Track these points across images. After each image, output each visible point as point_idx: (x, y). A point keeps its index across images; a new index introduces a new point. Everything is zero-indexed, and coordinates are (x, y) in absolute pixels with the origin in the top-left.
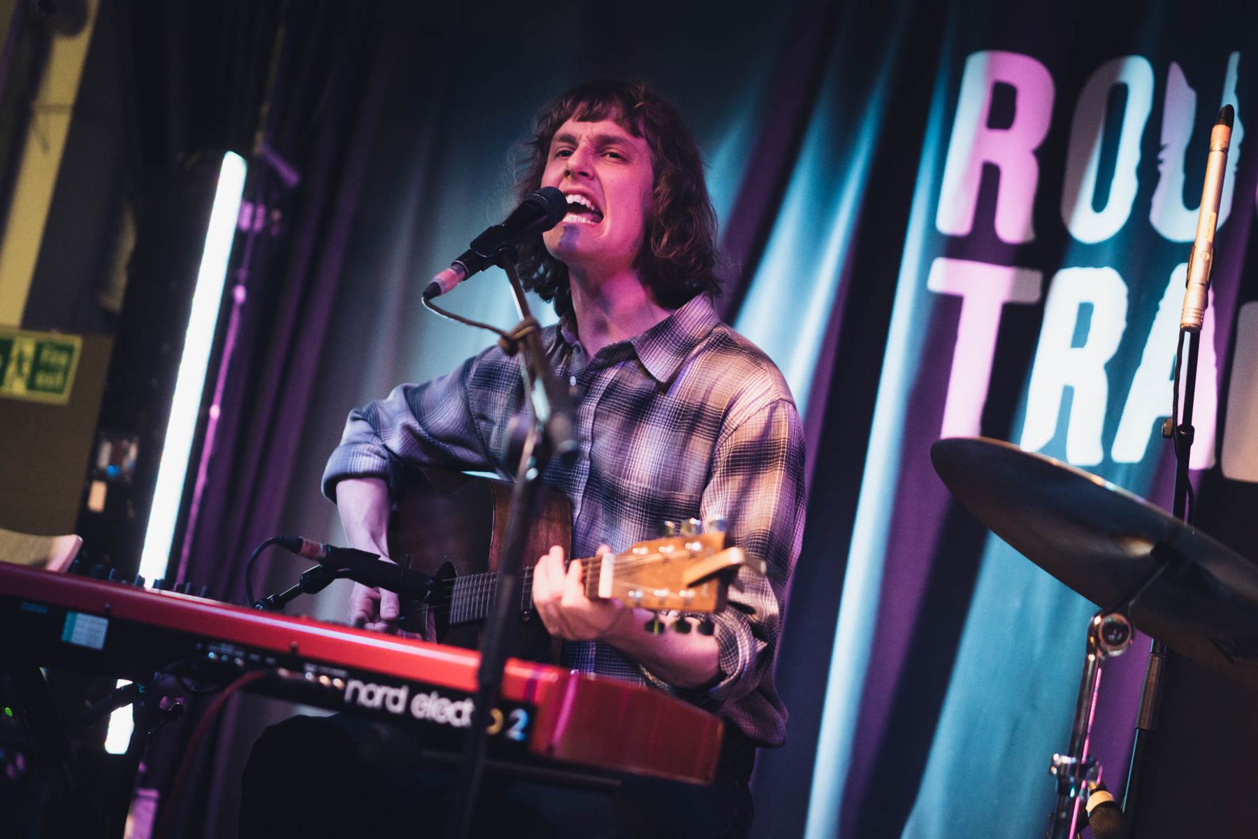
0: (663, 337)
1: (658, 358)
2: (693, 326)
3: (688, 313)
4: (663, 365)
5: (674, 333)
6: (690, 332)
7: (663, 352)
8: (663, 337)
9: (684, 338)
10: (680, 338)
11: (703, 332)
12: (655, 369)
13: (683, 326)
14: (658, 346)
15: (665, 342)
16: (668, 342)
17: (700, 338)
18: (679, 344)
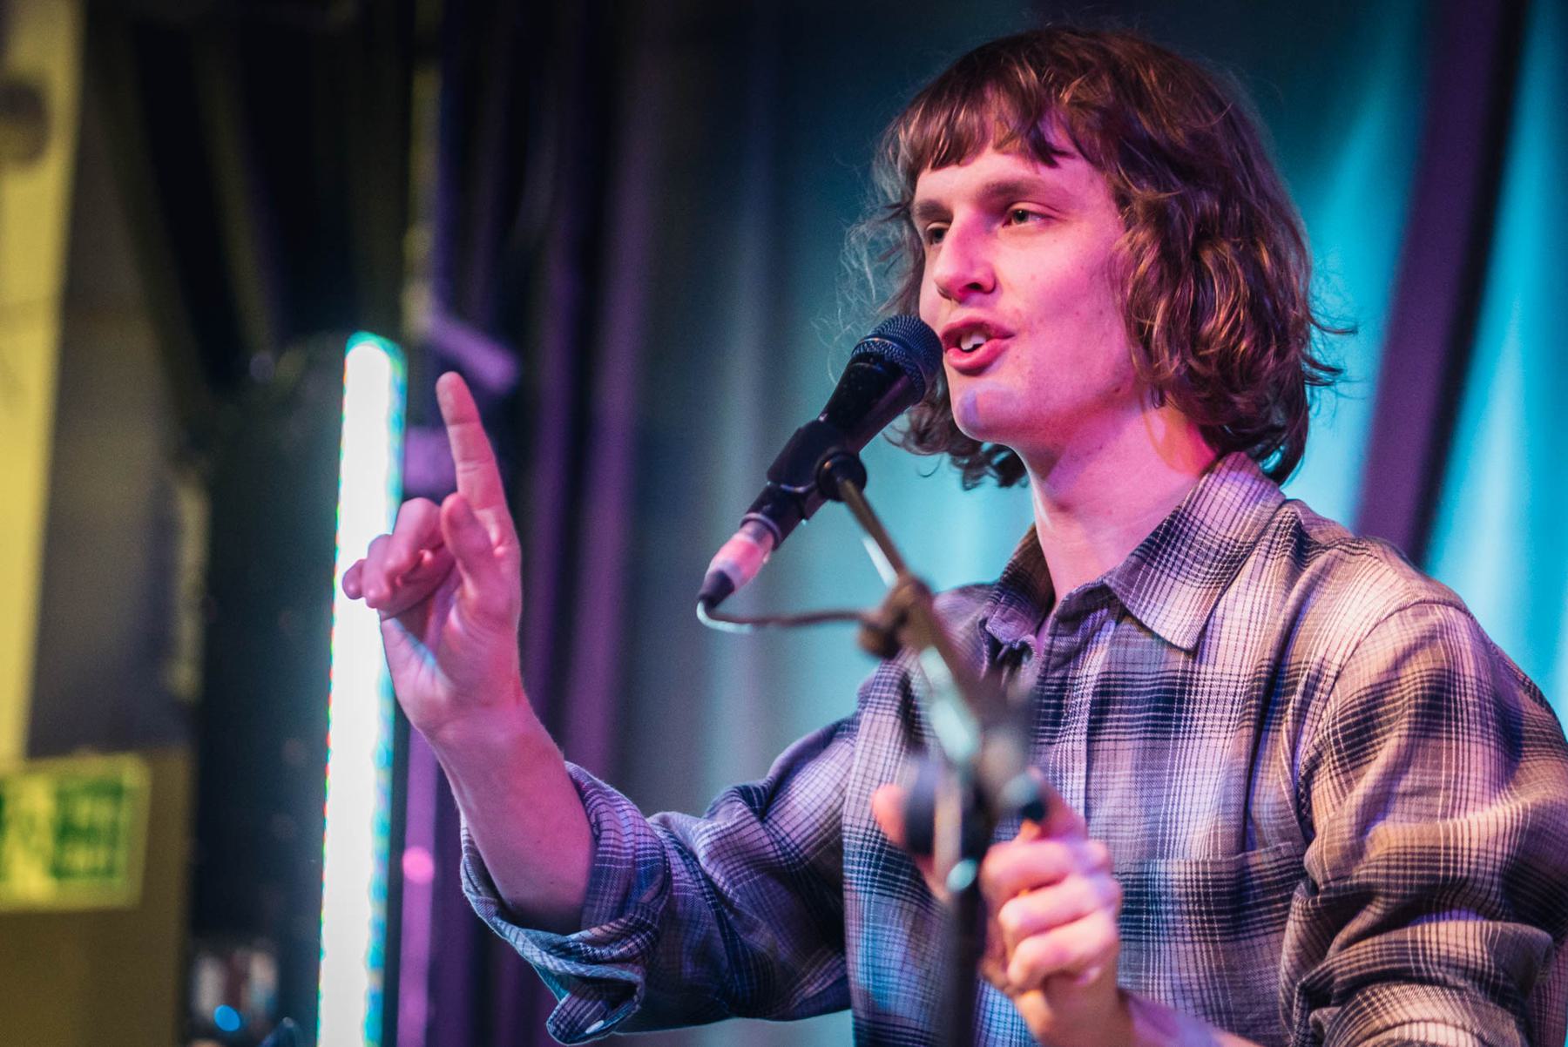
0: (1170, 555)
1: (1170, 600)
2: (1229, 517)
3: (1212, 494)
4: (1183, 612)
6: (1228, 530)
7: (1178, 585)
9: (1216, 547)
10: (1209, 549)
11: (1254, 525)
12: (1166, 625)
13: (1208, 521)
14: (1164, 577)
15: (1178, 563)
16: (1184, 562)
17: (1251, 539)
18: (1209, 562)
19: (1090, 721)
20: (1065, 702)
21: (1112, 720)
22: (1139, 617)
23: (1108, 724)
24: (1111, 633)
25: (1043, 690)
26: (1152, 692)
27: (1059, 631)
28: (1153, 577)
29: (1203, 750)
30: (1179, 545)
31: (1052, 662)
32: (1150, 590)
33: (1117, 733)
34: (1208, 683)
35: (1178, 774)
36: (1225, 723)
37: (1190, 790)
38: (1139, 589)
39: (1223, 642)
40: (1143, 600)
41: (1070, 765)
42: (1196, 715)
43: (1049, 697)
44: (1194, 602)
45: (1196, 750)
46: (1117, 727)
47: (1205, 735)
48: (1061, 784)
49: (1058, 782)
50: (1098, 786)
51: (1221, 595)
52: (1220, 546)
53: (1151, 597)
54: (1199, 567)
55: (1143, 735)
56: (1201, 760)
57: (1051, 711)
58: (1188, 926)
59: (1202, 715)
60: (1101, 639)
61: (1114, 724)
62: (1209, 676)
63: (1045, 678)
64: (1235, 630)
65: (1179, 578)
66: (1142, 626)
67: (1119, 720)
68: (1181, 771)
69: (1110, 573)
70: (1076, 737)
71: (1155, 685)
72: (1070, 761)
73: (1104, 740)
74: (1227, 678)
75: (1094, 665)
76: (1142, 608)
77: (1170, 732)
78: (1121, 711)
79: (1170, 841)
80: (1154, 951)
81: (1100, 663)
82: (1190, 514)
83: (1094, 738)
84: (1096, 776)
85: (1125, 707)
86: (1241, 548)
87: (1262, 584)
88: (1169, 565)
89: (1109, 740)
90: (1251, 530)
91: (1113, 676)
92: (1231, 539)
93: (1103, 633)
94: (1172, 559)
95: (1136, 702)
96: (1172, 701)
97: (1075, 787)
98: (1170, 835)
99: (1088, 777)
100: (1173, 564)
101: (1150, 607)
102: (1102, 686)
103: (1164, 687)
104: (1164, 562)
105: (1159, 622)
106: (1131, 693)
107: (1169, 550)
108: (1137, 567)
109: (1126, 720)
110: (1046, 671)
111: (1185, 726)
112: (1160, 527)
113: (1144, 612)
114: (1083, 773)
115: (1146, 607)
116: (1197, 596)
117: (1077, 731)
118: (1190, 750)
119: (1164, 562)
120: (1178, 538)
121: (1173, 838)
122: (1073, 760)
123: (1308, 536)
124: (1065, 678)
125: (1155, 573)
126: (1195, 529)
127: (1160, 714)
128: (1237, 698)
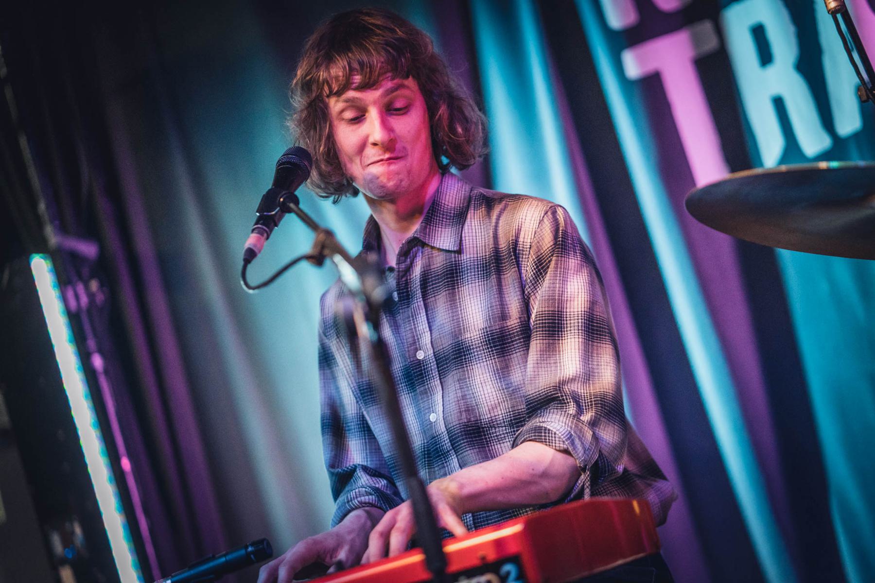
0: (437, 219)
1: (443, 235)
3: (445, 192)
5: (443, 212)
6: (455, 204)
7: (443, 230)
8: (437, 219)
9: (453, 212)
11: (464, 199)
12: (445, 245)
13: (446, 203)
14: (437, 229)
15: (441, 222)
16: (442, 221)
17: (465, 205)
19: (422, 292)
20: (409, 289)
21: (430, 289)
22: (433, 245)
23: (429, 291)
24: (420, 257)
25: (399, 287)
26: (444, 272)
27: (401, 262)
28: (433, 229)
29: (470, 289)
30: (438, 215)
31: (400, 275)
32: (433, 235)
33: (434, 293)
34: (465, 263)
35: (463, 301)
36: (477, 276)
37: (470, 305)
38: (429, 235)
39: (468, 246)
40: (432, 238)
41: (418, 312)
42: (464, 277)
43: (402, 289)
44: (452, 233)
45: (467, 290)
46: (433, 291)
47: (469, 283)
48: (417, 321)
49: (415, 320)
50: (432, 317)
51: (462, 227)
52: (454, 211)
53: (435, 237)
54: (449, 221)
55: (444, 290)
56: (471, 293)
57: (405, 294)
58: (484, 355)
59: (466, 275)
60: (417, 260)
61: (432, 290)
62: (465, 261)
63: (399, 282)
64: (471, 241)
65: (443, 227)
66: (433, 248)
67: (433, 288)
68: (464, 299)
69: (416, 232)
70: (418, 300)
71: (444, 269)
72: (418, 310)
73: (429, 298)
74: (473, 259)
75: (417, 271)
76: (433, 242)
77: (455, 286)
78: (433, 285)
79: (467, 327)
80: (470, 370)
81: (419, 268)
82: (439, 202)
83: (426, 298)
84: (430, 313)
85: (434, 282)
86: (462, 209)
87: (476, 220)
88: (438, 223)
89: (432, 297)
90: (464, 201)
91: (426, 272)
92: (457, 207)
93: (418, 258)
94: (438, 221)
95: (438, 279)
96: (453, 274)
97: (423, 320)
98: (466, 325)
99: (427, 315)
100: (439, 223)
101: (436, 240)
102: (422, 277)
103: (448, 269)
104: (435, 223)
105: (441, 244)
106: (435, 276)
107: (435, 218)
108: (426, 228)
109: (436, 287)
110: (399, 279)
111: (460, 282)
112: (429, 210)
113: (434, 243)
114: (425, 314)
115: (434, 241)
116: (453, 231)
117: (417, 298)
118: (465, 290)
119: (435, 223)
120: (437, 212)
121: (468, 326)
122: (419, 310)
123: (489, 198)
124: (407, 280)
125: (433, 228)
126: (443, 207)
127: (449, 280)
128: (479, 266)
